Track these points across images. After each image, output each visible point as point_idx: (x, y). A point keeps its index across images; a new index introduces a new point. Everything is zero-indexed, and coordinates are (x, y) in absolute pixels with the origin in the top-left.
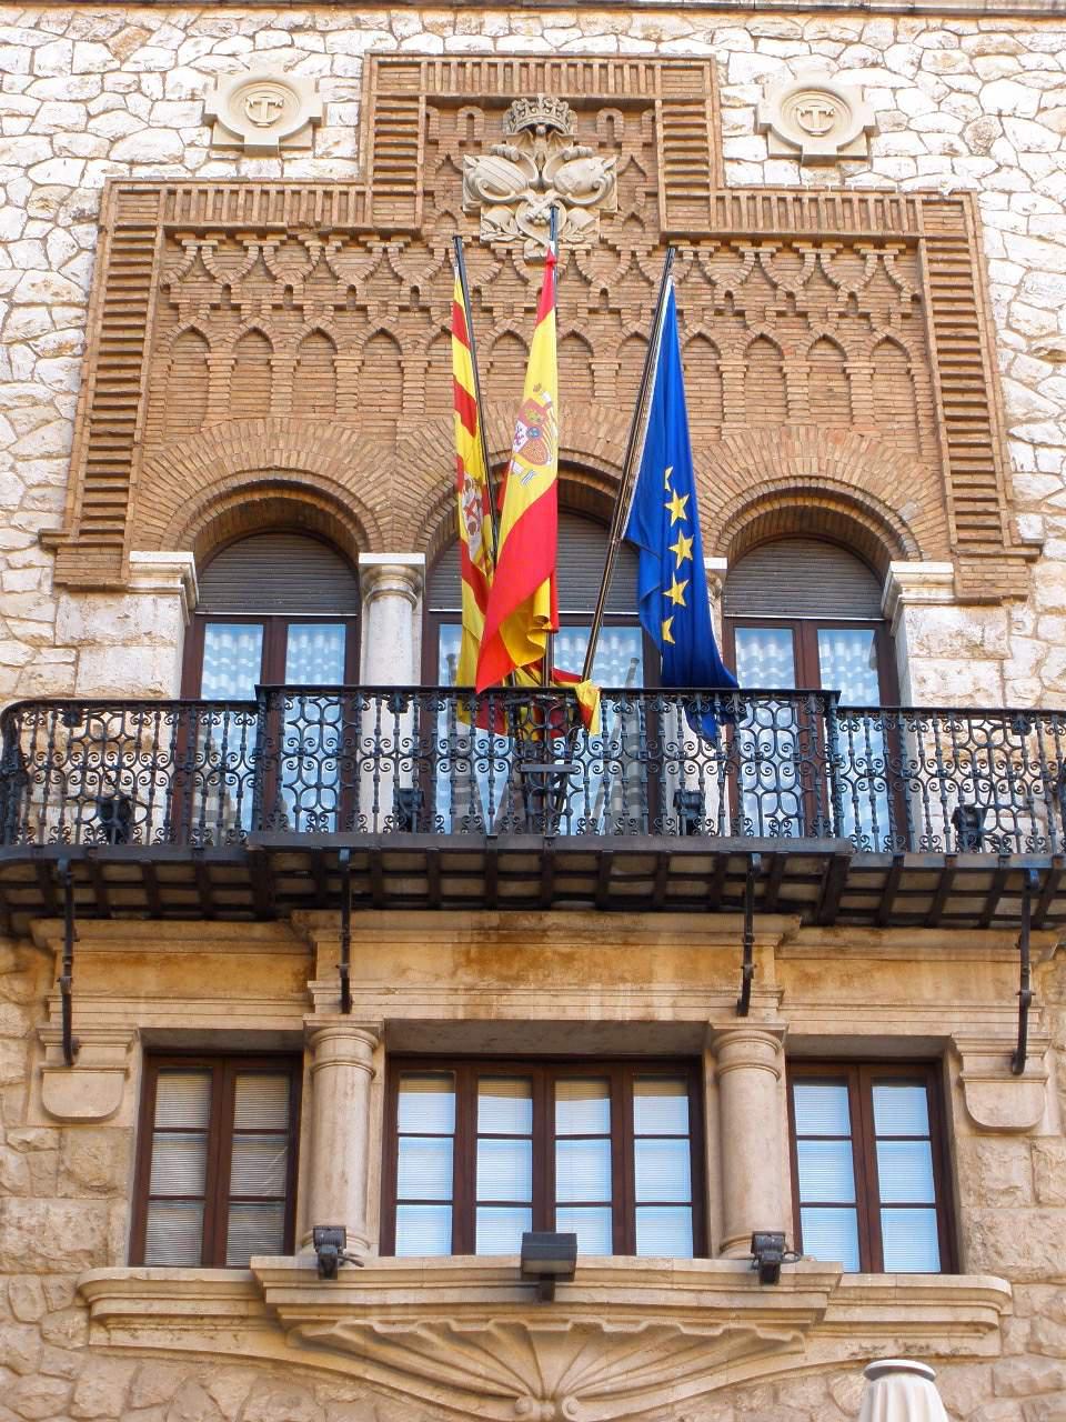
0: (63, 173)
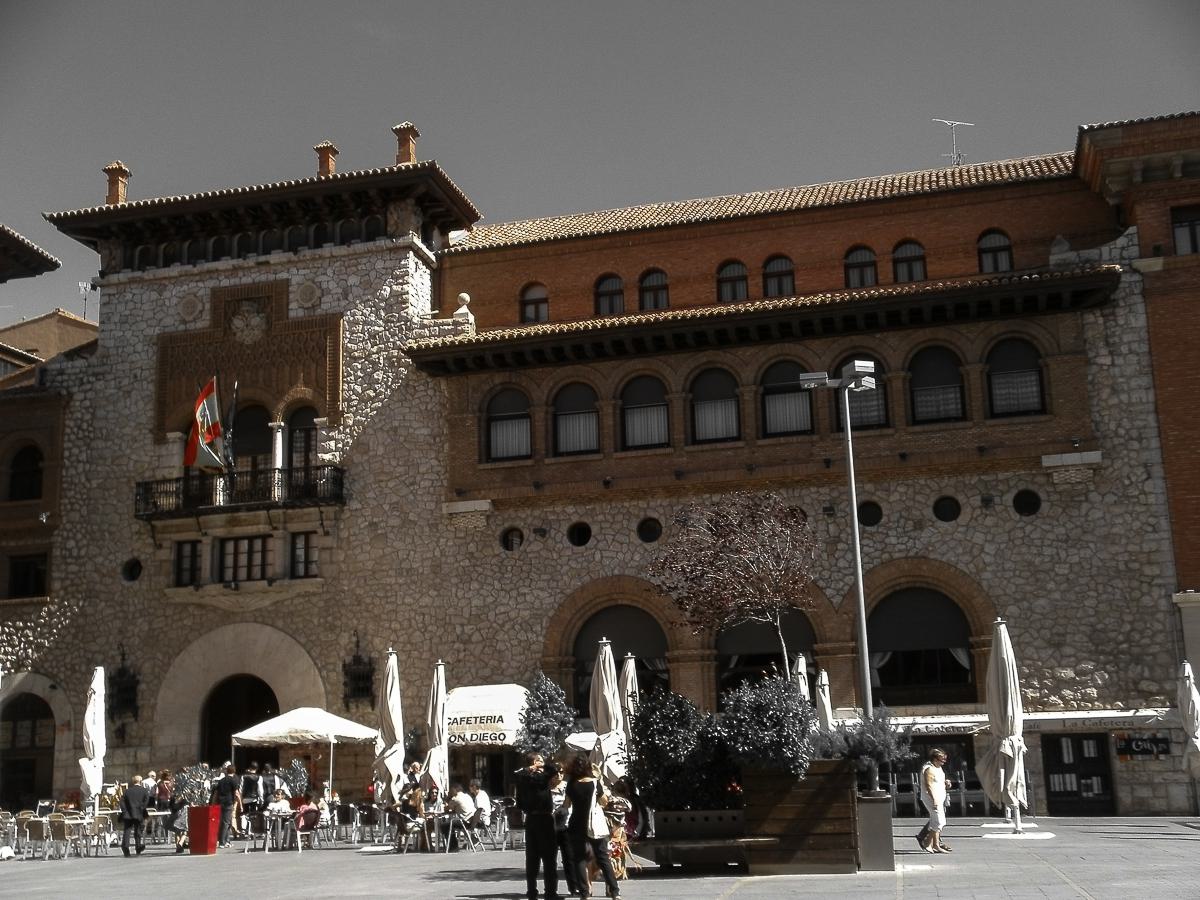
0: (150, 332)
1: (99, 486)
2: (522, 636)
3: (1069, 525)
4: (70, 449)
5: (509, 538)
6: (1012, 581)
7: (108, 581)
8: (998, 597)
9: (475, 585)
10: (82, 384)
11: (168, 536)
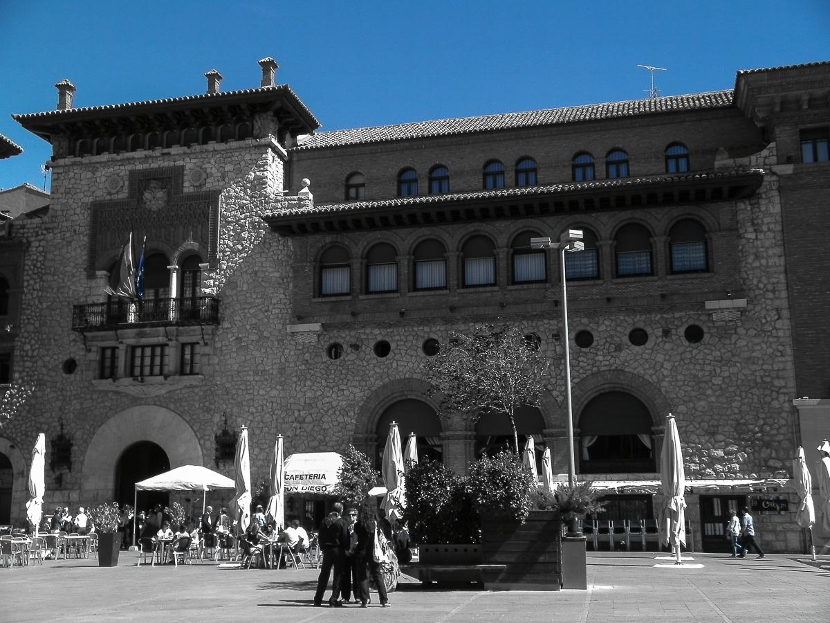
0: (86, 200)
1: (48, 307)
2: (341, 419)
3: (723, 351)
4: (28, 281)
5: (335, 351)
6: (683, 388)
7: (53, 374)
8: (672, 399)
9: (308, 383)
10: (38, 235)
11: (94, 343)
